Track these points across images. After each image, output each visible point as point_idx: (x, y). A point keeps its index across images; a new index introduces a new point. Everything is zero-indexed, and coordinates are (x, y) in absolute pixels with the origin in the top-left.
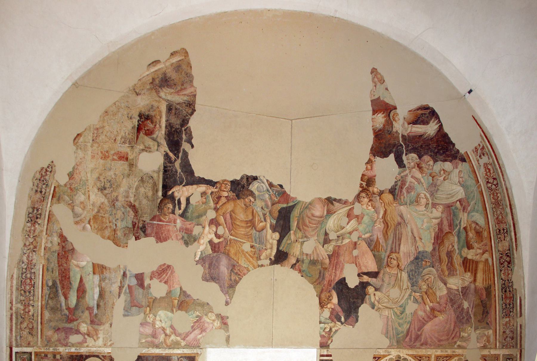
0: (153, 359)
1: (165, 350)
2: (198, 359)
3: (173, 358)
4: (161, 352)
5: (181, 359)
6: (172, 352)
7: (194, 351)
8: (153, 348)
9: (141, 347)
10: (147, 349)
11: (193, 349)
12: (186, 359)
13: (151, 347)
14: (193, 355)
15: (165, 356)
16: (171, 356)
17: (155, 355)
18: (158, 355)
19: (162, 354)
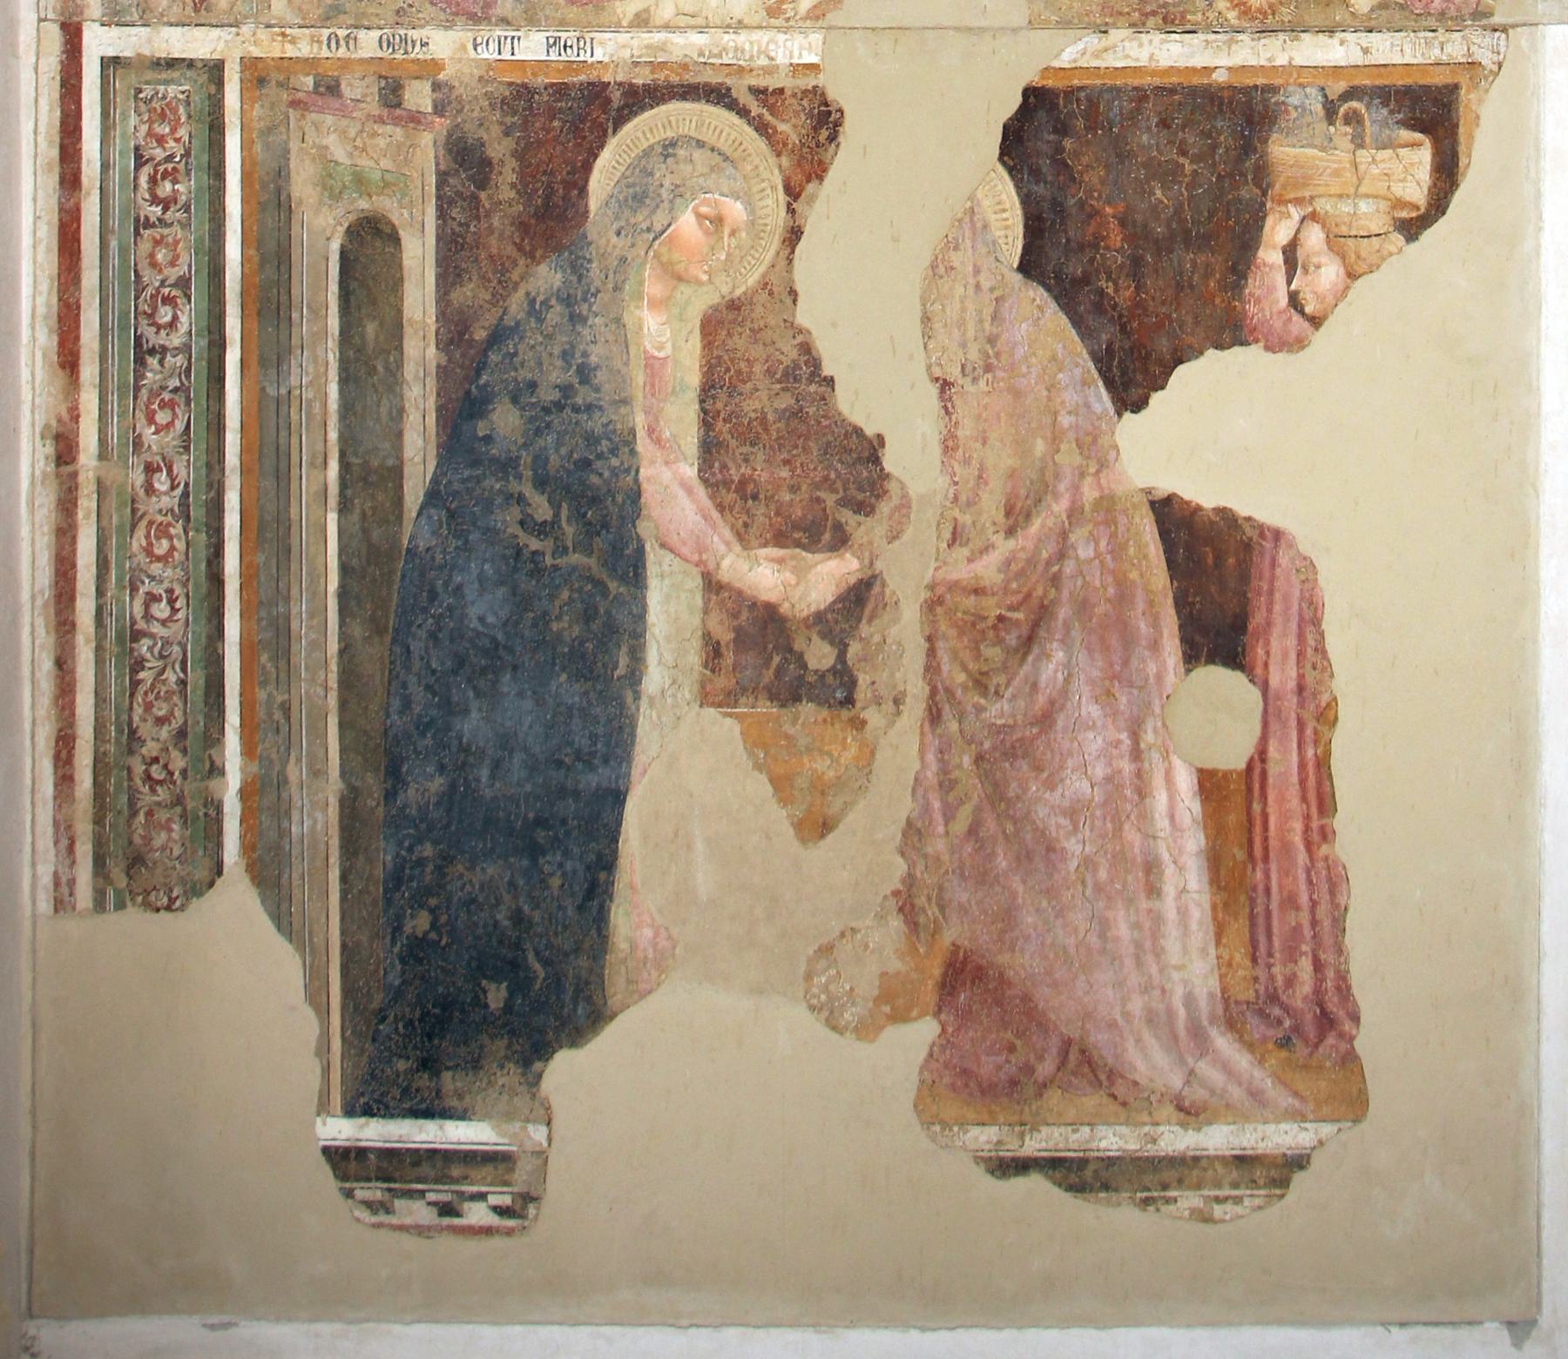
0: (1138, 110)
1: (1230, 43)
2: (1480, 101)
3: (1294, 100)
4: (1199, 61)
5: (1354, 104)
6: (1281, 60)
7: (1448, 49)
8: (1138, 27)
9: (1044, 25)
10: (1092, 41)
11: (1441, 35)
12: (1385, 104)
13: (1122, 21)
14: (1439, 79)
15: (1231, 87)
16: (1273, 89)
17: (1157, 81)
18: (1175, 80)
19: (1208, 70)
